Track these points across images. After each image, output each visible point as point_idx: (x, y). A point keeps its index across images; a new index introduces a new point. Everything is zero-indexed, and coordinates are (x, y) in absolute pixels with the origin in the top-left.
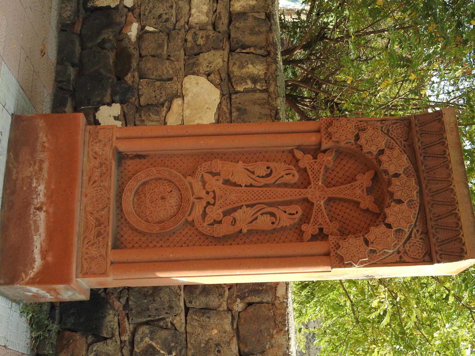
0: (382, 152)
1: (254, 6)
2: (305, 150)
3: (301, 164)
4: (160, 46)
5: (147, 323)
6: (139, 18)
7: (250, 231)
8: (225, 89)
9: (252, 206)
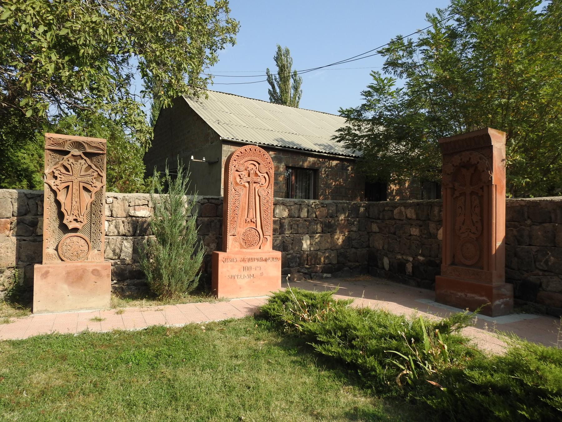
0: (453, 165)
5: (535, 262)
6: (417, 255)
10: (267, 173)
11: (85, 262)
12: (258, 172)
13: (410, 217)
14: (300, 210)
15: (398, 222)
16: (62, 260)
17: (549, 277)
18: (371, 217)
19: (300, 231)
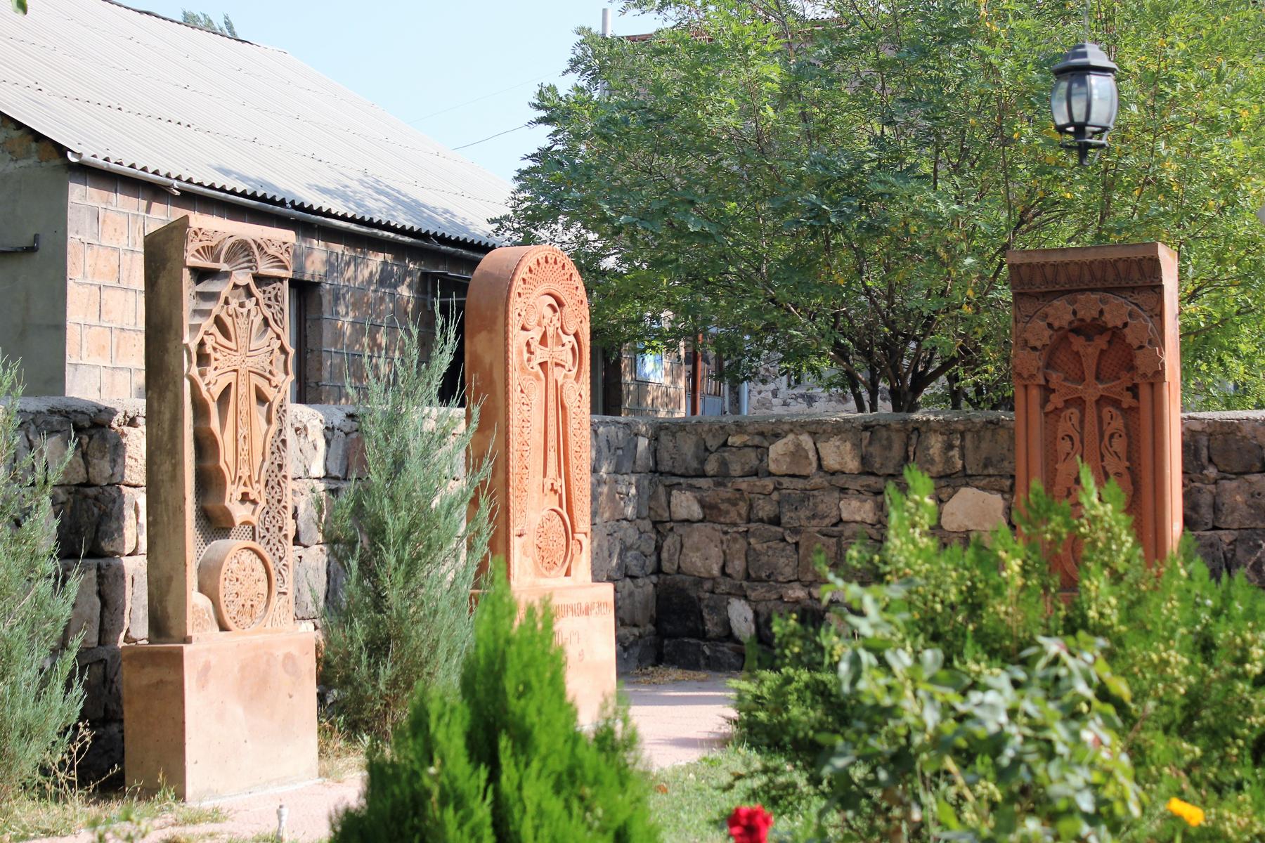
0: (1050, 326)
1: (853, 445)
2: (1045, 401)
3: (1060, 405)
7: (1129, 459)
8: (959, 482)
9: (1102, 456)
13: (837, 467)
15: (786, 482)
16: (223, 627)
18: (665, 466)
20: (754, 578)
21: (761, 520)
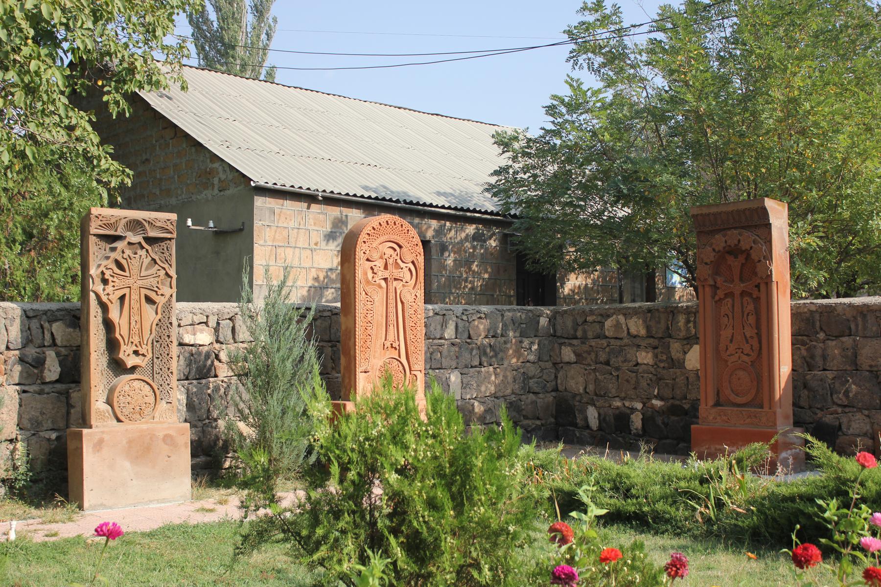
0: (714, 250)
4: (667, 385)
5: (831, 395)
6: (649, 399)
10: (413, 262)
11: (152, 423)
12: (399, 261)
13: (635, 333)
14: (444, 325)
15: (612, 341)
16: (119, 420)
17: (850, 414)
18: (559, 334)
19: (445, 363)
20: (599, 395)
21: (601, 363)
